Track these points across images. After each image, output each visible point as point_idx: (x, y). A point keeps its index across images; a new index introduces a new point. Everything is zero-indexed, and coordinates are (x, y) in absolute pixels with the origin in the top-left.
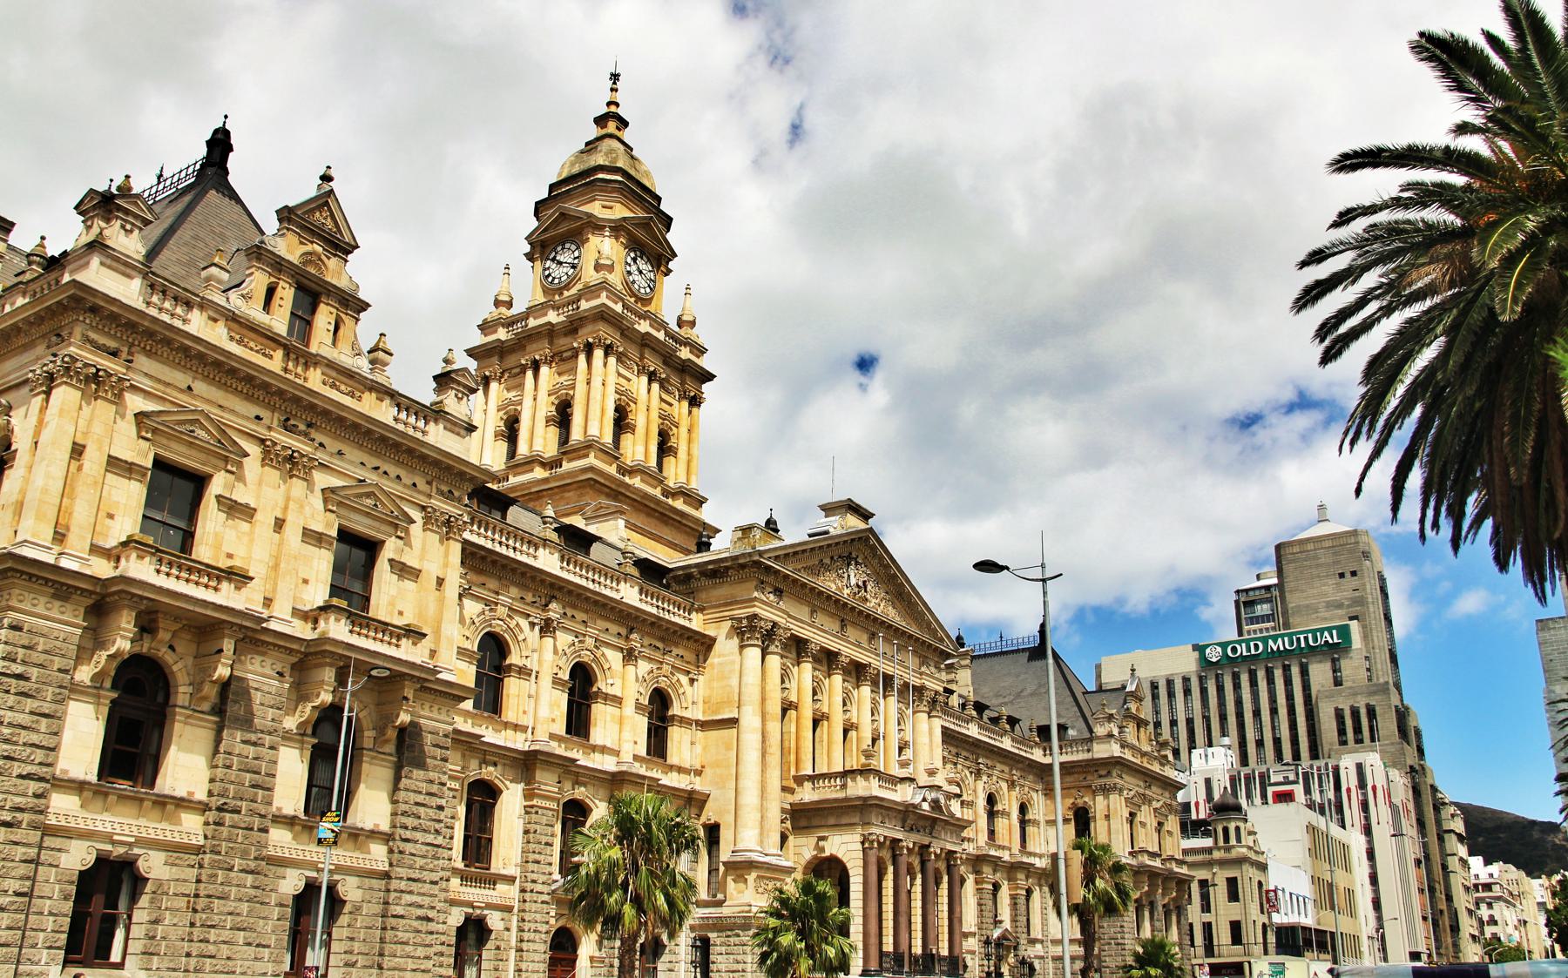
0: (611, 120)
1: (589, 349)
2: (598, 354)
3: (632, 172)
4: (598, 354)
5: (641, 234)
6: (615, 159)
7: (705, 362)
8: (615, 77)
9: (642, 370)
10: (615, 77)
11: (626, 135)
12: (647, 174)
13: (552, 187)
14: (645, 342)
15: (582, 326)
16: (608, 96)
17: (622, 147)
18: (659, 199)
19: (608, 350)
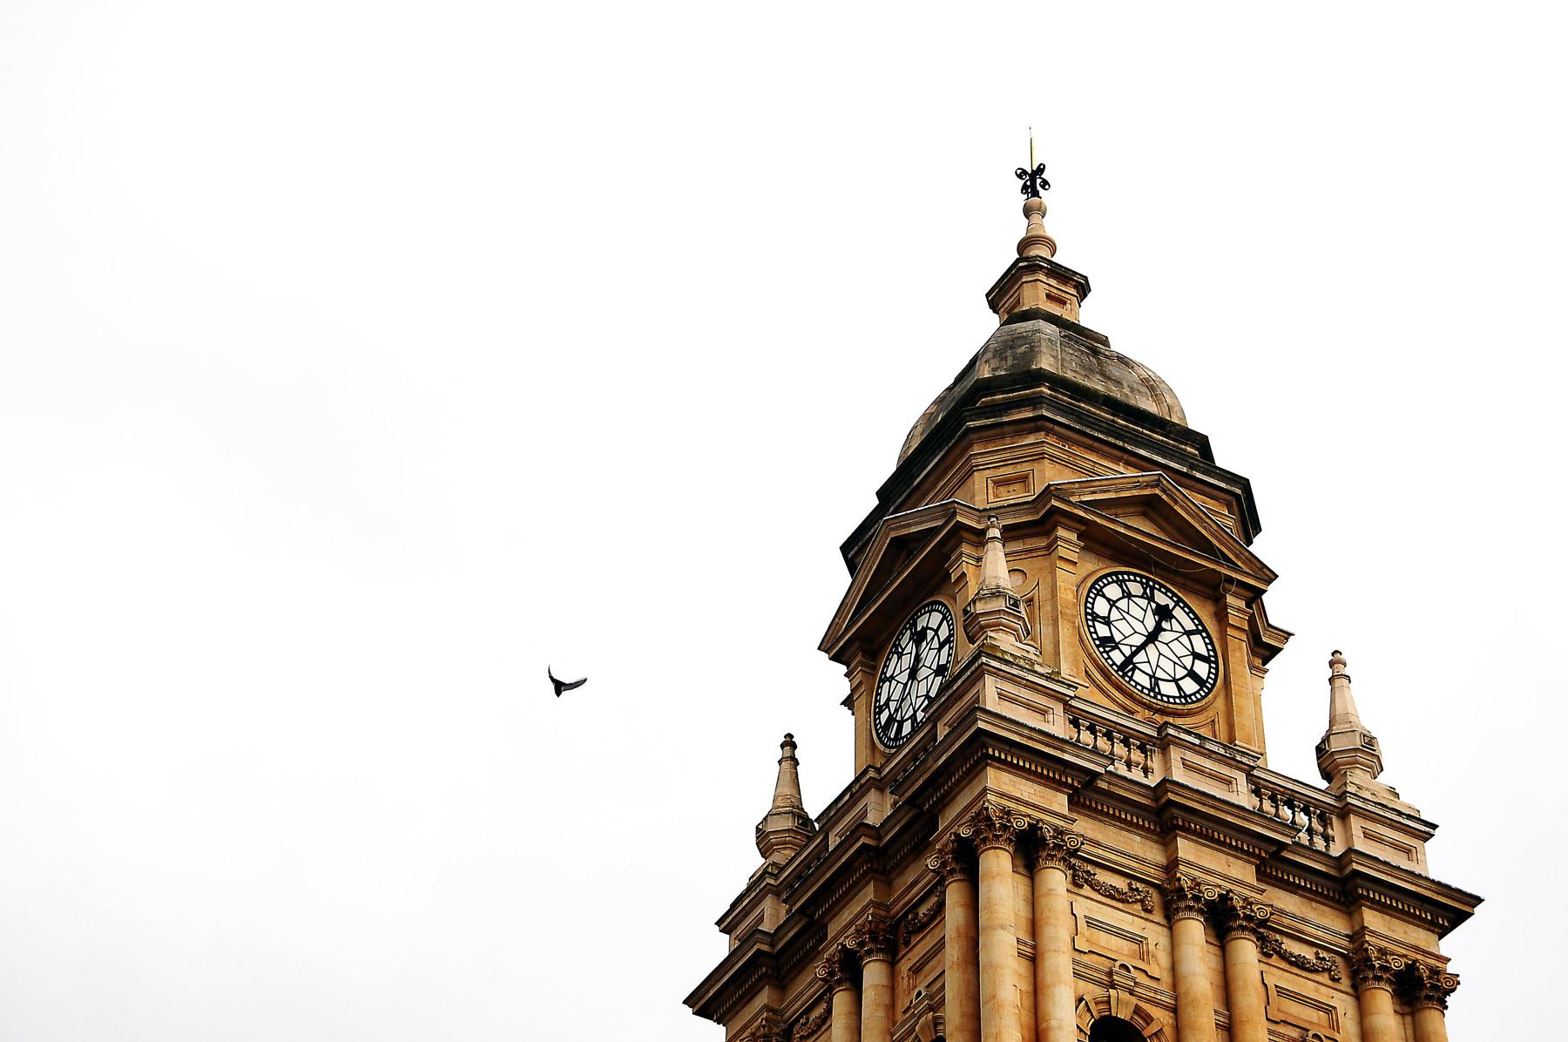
0: (1033, 282)
1: (966, 861)
2: (998, 864)
3: (1097, 384)
4: (998, 864)
5: (1140, 528)
6: (1032, 353)
7: (1441, 862)
8: (1033, 181)
9: (1171, 899)
10: (1033, 181)
11: (1089, 315)
12: (1152, 386)
13: (880, 494)
14: (1164, 815)
15: (945, 802)
16: (1019, 228)
17: (1050, 329)
18: (1202, 443)
19: (1032, 849)
